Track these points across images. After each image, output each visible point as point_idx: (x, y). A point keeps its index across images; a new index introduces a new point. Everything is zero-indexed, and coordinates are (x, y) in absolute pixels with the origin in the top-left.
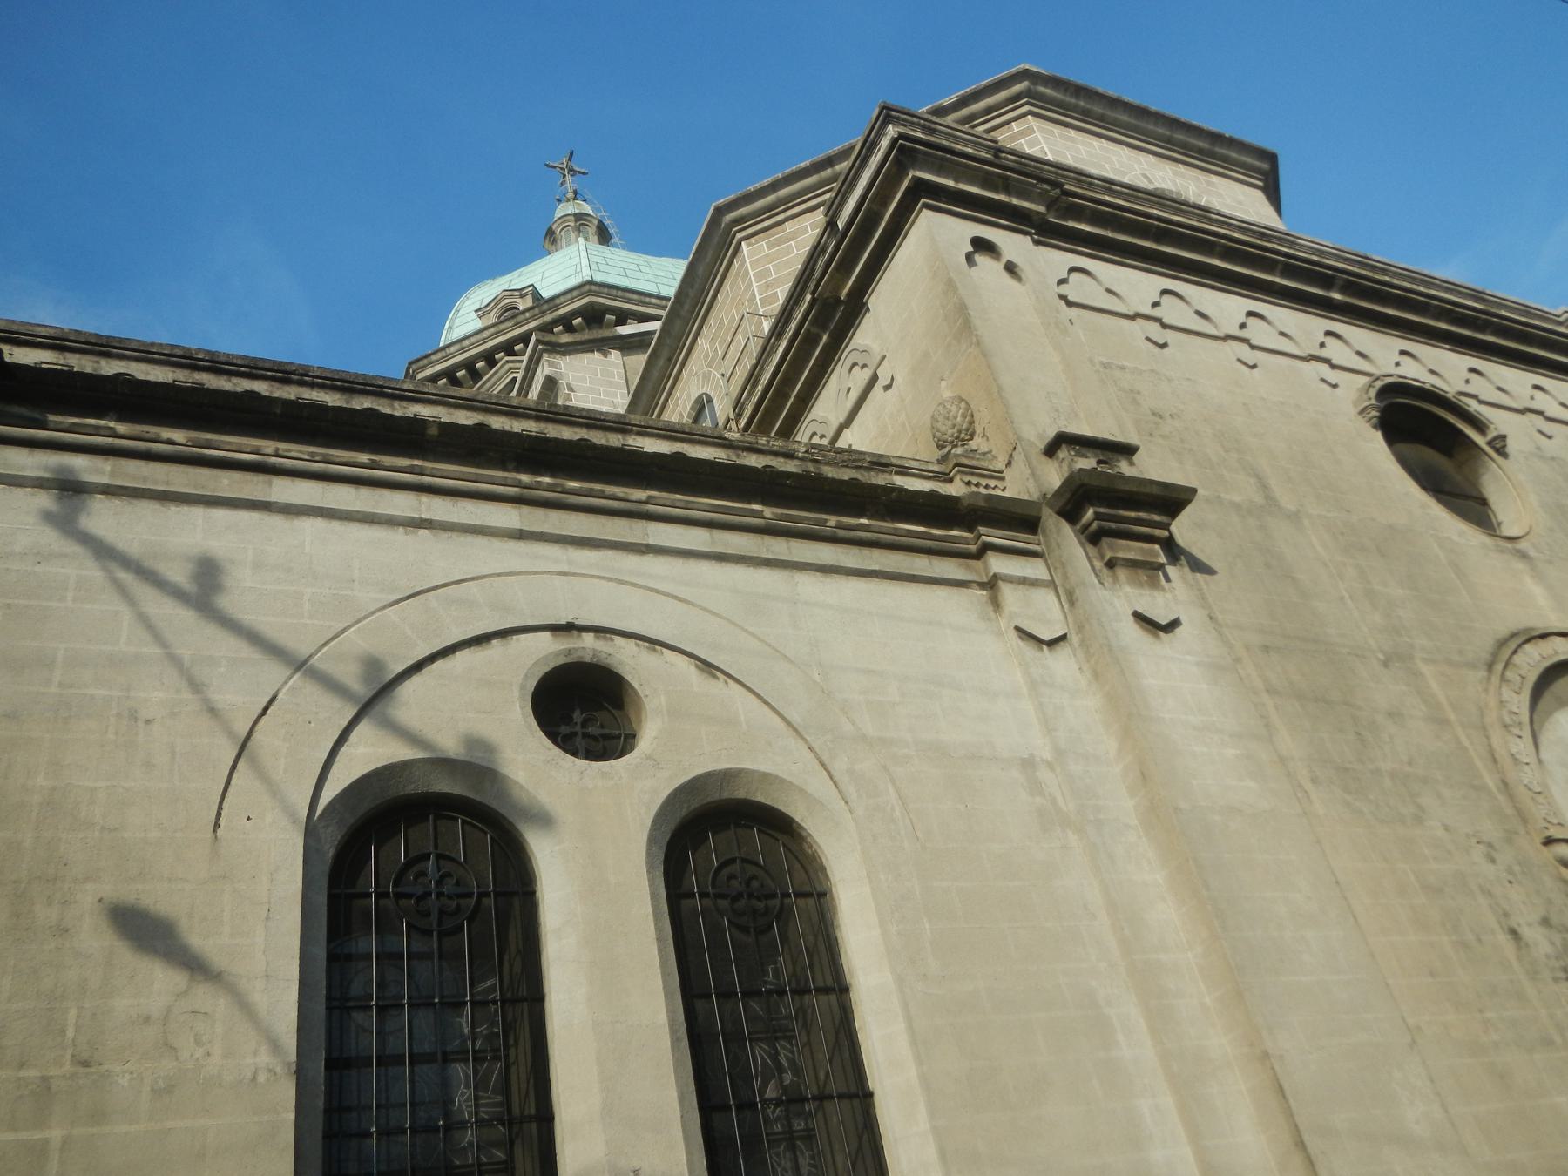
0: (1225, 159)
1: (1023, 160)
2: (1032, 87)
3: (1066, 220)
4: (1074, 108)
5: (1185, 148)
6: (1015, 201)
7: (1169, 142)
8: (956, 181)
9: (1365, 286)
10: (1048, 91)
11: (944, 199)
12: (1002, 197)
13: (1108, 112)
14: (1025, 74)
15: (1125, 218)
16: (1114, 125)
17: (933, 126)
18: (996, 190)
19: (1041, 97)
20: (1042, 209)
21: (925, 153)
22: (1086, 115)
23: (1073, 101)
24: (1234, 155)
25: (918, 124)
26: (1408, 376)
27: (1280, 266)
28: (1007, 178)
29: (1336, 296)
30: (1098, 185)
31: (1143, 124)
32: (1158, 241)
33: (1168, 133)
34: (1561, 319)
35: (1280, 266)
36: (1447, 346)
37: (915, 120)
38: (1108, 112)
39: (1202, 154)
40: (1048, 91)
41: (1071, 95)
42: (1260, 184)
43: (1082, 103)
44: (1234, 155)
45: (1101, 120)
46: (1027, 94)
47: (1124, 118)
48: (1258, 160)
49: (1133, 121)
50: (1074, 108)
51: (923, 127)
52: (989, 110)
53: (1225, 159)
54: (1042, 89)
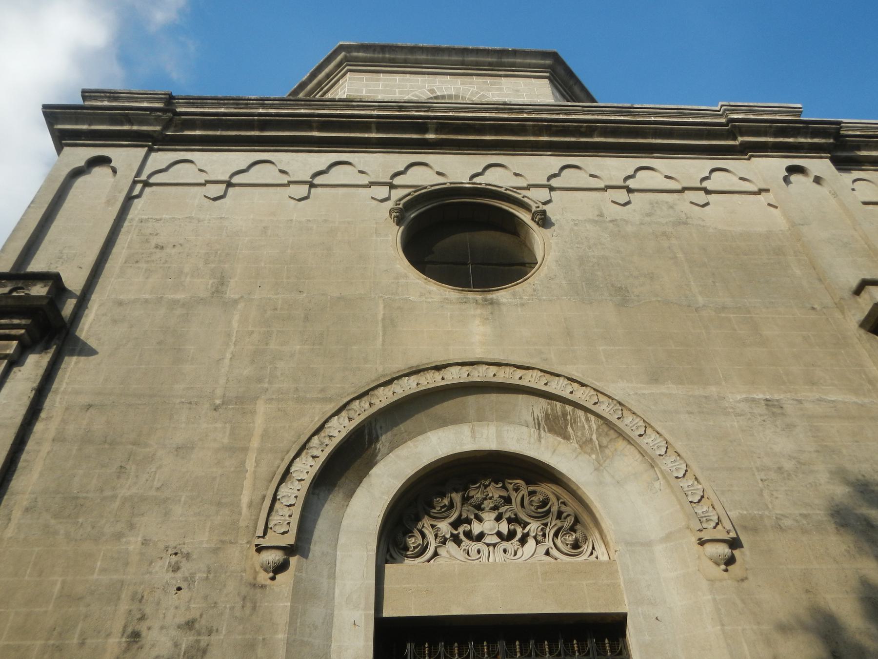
0: (513, 65)
1: (191, 101)
2: (348, 55)
3: (183, 131)
4: (383, 60)
5: (478, 66)
6: (135, 128)
7: (463, 64)
8: (90, 125)
9: (457, 124)
10: (361, 54)
11: (83, 138)
12: (126, 128)
13: (409, 57)
14: (341, 48)
15: (230, 120)
16: (417, 63)
17: (116, 95)
18: (122, 124)
19: (356, 59)
20: (158, 128)
21: (62, 113)
22: (393, 62)
23: (381, 56)
24: (519, 61)
25: (106, 97)
26: (478, 182)
27: (373, 125)
28: (127, 115)
29: (431, 136)
30: (253, 104)
31: (439, 58)
32: (262, 129)
33: (460, 59)
34: (720, 113)
35: (373, 125)
36: (549, 153)
37: (102, 94)
38: (409, 57)
39: (492, 66)
40: (361, 54)
41: (379, 53)
42: (548, 74)
43: (387, 56)
44: (519, 61)
45: (405, 63)
46: (346, 59)
47: (423, 57)
48: (541, 60)
49: (429, 57)
50: (383, 60)
51: (109, 97)
52: (328, 76)
53: (513, 65)
54: (355, 54)
